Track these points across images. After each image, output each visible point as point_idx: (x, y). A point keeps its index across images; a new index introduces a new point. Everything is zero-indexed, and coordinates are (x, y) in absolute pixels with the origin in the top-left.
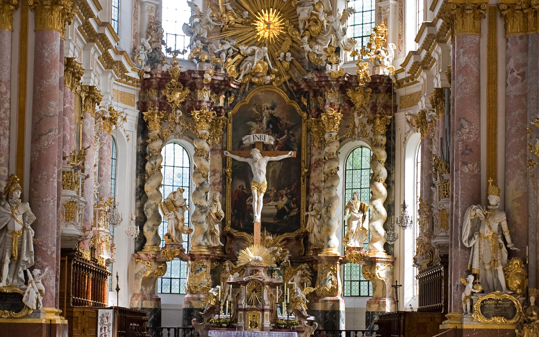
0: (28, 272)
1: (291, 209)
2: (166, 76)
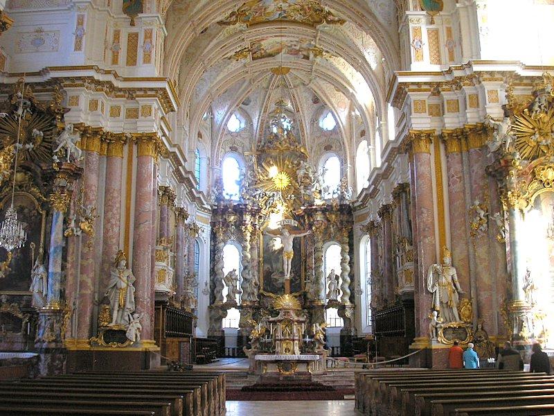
0: (130, 316)
2: (226, 208)
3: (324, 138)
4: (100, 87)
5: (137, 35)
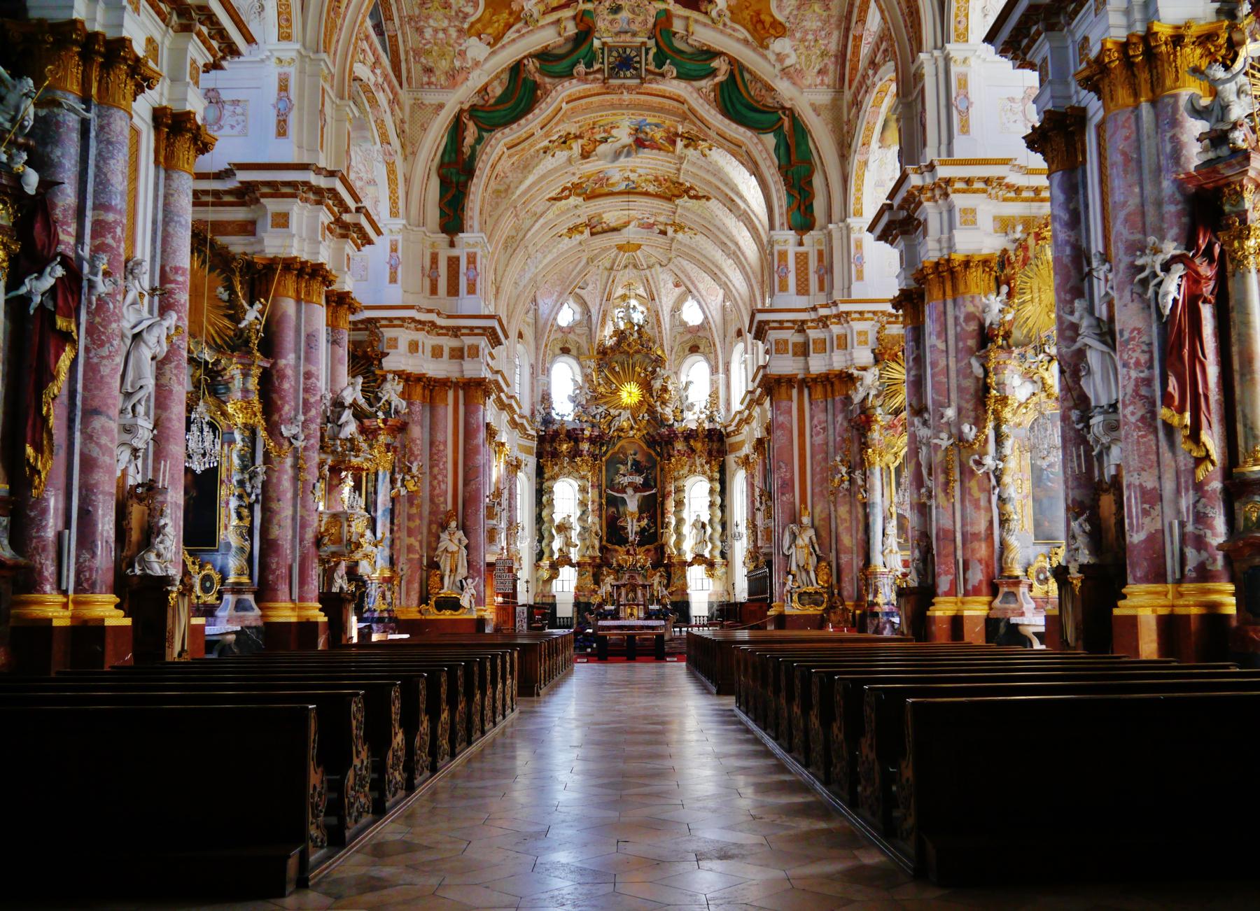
1: (650, 528)
2: (557, 433)
3: (689, 336)
4: (420, 326)
5: (458, 259)
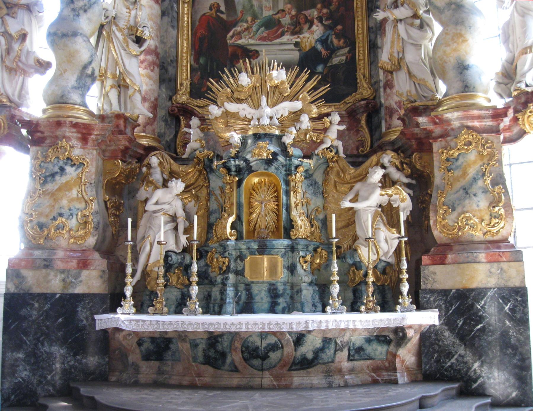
1: (332, 51)
